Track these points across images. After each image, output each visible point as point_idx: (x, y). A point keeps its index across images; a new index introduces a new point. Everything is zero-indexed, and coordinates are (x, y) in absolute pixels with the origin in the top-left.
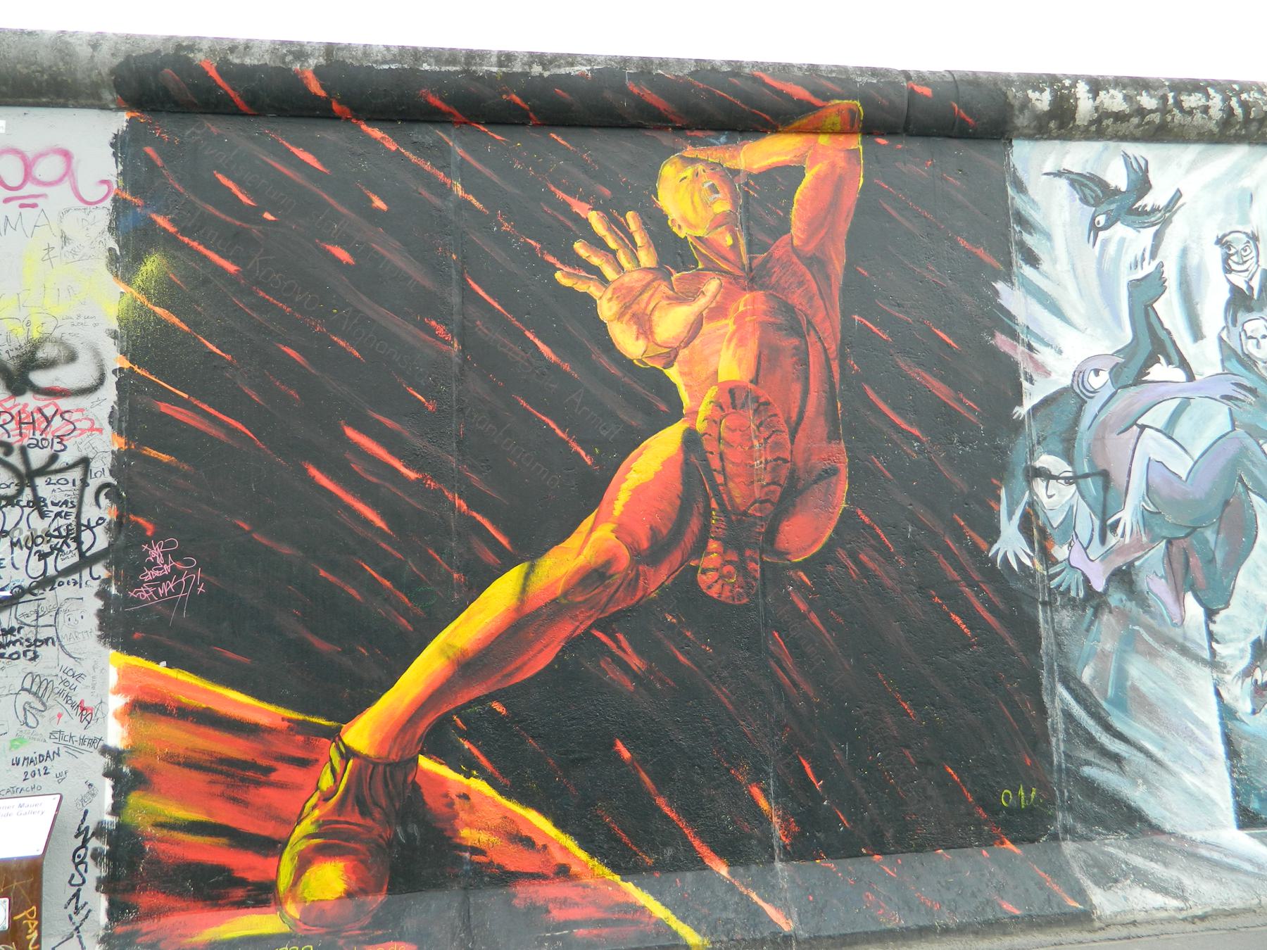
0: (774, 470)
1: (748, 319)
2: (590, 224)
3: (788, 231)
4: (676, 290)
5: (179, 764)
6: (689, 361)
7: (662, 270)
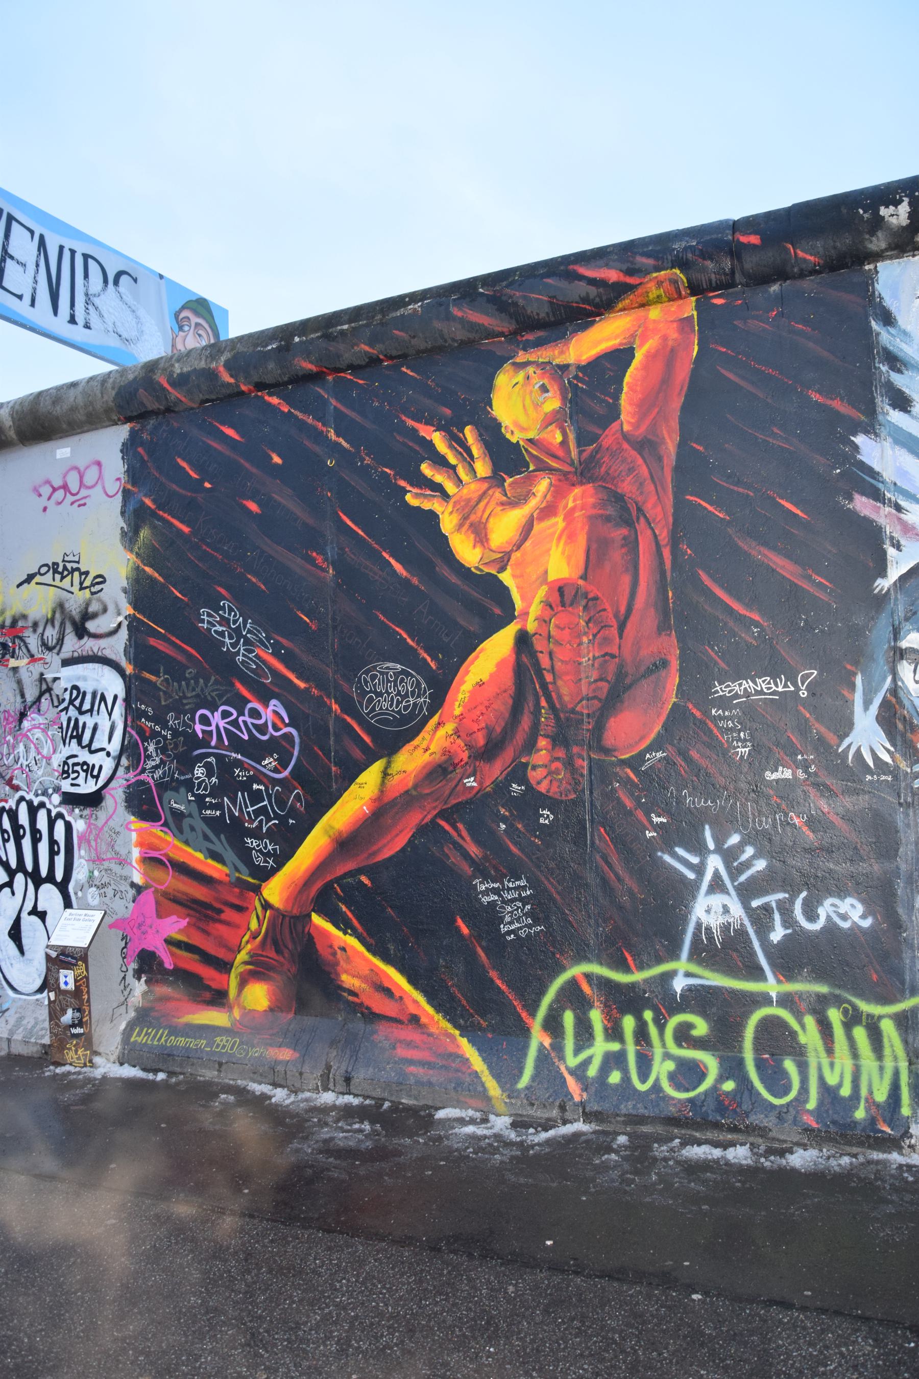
0: (603, 666)
1: (577, 514)
2: (434, 445)
3: (618, 417)
4: (509, 495)
5: (170, 900)
6: (518, 564)
7: (495, 479)
